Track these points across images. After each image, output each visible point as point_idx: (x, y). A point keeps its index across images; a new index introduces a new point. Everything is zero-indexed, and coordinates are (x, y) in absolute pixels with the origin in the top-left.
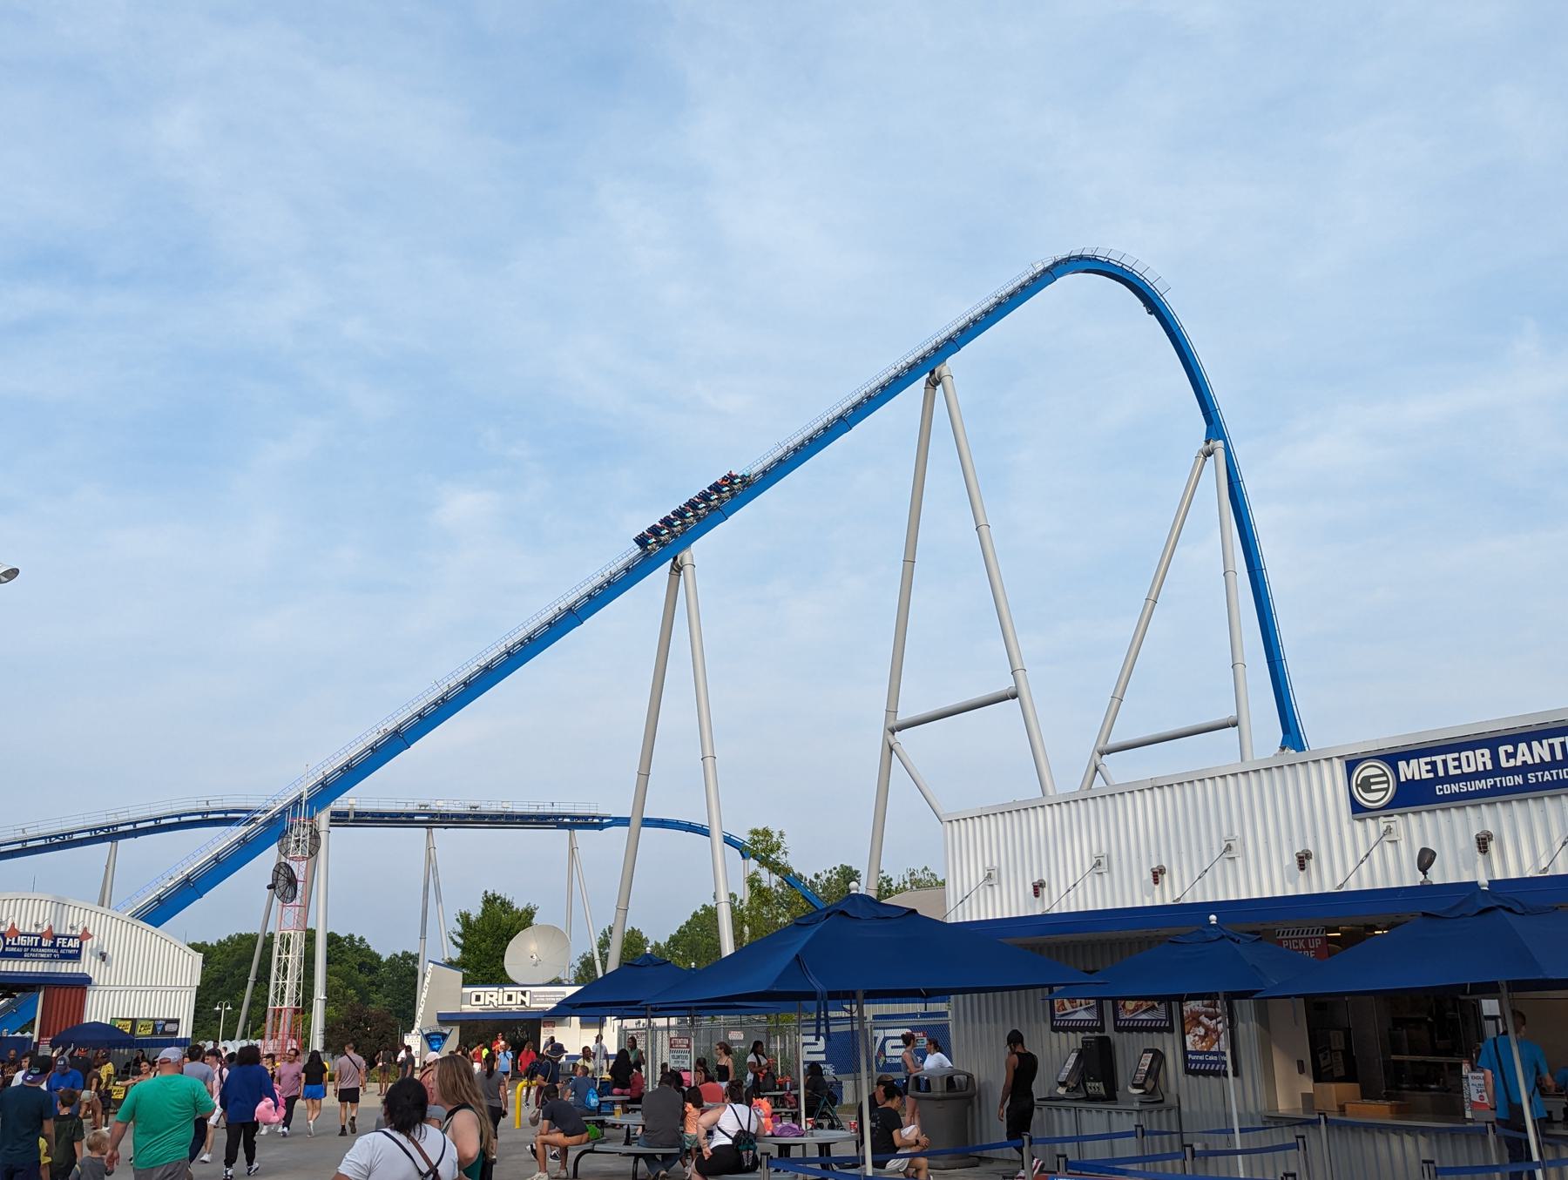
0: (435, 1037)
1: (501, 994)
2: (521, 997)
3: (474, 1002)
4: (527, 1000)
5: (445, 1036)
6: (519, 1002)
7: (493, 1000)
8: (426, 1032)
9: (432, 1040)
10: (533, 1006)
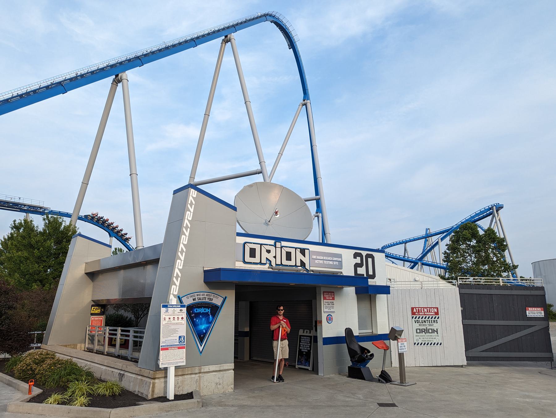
0: (202, 310)
1: (278, 250)
2: (300, 256)
3: (248, 259)
4: (306, 260)
5: (215, 310)
6: (299, 264)
7: (270, 256)
8: (188, 301)
9: (198, 315)
10: (312, 268)
